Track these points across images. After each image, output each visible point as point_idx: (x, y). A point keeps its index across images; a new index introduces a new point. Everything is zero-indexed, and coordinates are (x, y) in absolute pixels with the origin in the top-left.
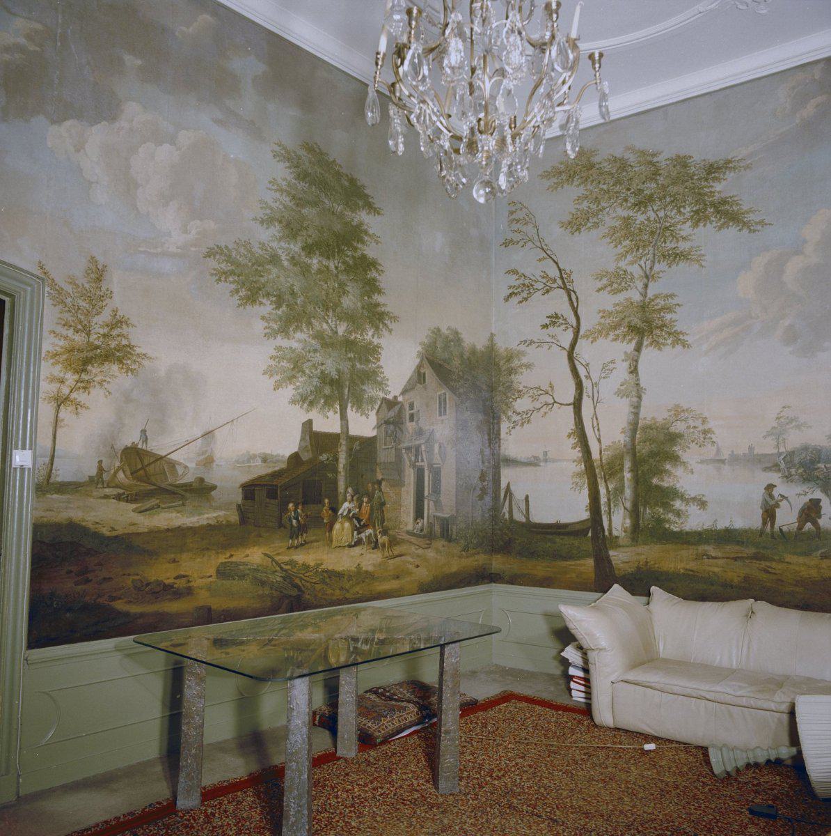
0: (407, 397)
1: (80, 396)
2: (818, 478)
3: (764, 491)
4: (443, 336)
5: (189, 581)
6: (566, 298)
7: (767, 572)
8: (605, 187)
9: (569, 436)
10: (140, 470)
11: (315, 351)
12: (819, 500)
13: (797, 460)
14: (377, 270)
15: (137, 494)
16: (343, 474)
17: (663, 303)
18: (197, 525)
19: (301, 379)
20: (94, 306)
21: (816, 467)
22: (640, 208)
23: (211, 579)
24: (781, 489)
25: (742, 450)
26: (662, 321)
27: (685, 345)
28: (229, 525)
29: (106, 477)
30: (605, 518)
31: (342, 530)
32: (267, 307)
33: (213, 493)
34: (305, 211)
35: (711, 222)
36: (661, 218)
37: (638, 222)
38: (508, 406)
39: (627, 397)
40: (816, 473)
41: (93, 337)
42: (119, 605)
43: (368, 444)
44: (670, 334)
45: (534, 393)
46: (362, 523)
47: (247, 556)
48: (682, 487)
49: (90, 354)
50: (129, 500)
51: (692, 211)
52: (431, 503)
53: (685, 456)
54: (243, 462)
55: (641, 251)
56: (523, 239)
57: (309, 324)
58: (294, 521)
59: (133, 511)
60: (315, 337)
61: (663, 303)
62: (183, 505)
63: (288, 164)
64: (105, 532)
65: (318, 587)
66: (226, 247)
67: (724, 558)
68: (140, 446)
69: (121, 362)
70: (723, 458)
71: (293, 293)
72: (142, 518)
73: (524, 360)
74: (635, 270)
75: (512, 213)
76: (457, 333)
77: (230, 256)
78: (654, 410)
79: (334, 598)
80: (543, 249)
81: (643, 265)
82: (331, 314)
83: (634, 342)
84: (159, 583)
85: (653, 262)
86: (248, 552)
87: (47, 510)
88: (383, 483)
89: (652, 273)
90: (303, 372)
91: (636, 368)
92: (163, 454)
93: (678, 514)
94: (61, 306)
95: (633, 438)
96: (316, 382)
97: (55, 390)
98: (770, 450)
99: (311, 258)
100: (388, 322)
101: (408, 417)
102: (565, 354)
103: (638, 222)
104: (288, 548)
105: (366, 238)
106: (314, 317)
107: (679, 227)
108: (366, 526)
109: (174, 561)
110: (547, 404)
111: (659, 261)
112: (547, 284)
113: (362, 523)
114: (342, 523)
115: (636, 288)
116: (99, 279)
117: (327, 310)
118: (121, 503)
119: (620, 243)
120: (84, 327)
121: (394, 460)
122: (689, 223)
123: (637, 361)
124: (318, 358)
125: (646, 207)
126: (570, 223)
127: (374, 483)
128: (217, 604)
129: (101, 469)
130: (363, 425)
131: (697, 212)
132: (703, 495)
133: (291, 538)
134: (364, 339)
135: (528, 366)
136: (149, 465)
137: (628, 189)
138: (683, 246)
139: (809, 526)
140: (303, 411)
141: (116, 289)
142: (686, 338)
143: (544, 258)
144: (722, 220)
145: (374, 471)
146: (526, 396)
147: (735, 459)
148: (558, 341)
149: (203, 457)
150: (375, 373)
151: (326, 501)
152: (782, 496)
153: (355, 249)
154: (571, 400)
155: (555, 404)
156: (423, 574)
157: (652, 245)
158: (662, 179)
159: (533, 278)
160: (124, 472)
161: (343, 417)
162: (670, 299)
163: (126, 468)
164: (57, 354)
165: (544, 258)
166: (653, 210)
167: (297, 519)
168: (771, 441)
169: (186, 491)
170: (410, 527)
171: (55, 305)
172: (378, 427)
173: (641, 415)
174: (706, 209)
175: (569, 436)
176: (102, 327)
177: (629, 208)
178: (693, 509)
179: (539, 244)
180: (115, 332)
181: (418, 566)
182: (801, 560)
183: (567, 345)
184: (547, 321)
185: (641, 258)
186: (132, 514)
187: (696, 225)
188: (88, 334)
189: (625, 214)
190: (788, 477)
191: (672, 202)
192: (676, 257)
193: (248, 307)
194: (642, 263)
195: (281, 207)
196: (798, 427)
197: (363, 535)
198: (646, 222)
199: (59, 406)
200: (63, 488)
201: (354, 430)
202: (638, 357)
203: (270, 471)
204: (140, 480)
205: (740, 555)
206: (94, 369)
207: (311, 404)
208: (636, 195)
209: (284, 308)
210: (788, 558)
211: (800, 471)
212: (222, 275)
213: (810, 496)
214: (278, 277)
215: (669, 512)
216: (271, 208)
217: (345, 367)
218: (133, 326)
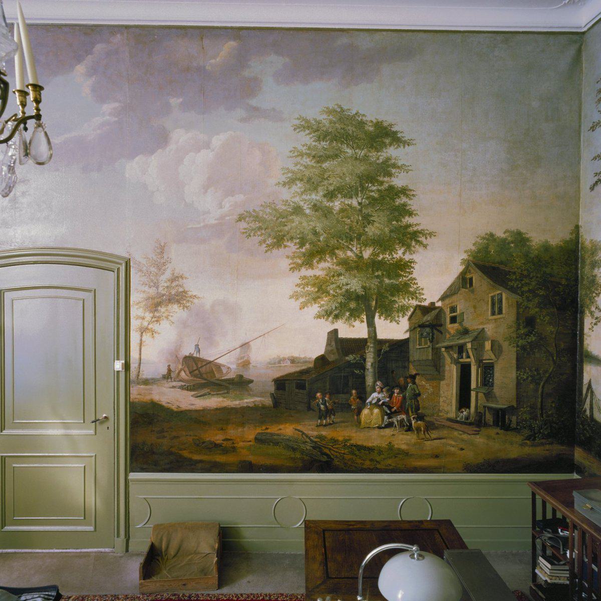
0: (447, 301)
1: (155, 326)
5: (233, 443)
10: (195, 370)
15: (194, 386)
16: (371, 370)
18: (239, 407)
19: (326, 299)
23: (250, 443)
28: (264, 407)
29: (173, 375)
32: (292, 247)
33: (250, 385)
34: (326, 165)
41: (161, 289)
42: (185, 454)
43: (399, 347)
47: (280, 429)
49: (159, 300)
50: (188, 389)
52: (480, 395)
57: (333, 254)
58: (322, 406)
59: (192, 396)
60: (338, 264)
62: (227, 393)
63: (307, 132)
64: (174, 408)
65: (347, 457)
66: (254, 211)
71: (315, 233)
72: (198, 400)
77: (257, 217)
79: (364, 467)
82: (355, 243)
84: (211, 443)
86: (281, 427)
88: (418, 377)
92: (211, 359)
97: (139, 324)
99: (332, 202)
105: (393, 171)
106: (338, 249)
114: (371, 410)
116: (162, 253)
118: (184, 391)
121: (430, 358)
124: (343, 280)
129: (169, 371)
130: (394, 329)
133: (320, 418)
136: (202, 367)
149: (242, 360)
156: (469, 455)
160: (184, 371)
161: (371, 324)
163: (186, 369)
164: (140, 302)
167: (325, 404)
169: (229, 384)
170: (452, 415)
172: (411, 330)
176: (166, 282)
180: (174, 284)
181: (462, 449)
188: (157, 288)
193: (275, 251)
195: (301, 168)
197: (394, 420)
199: (142, 333)
200: (146, 382)
201: (381, 335)
204: (195, 376)
206: (162, 309)
207: (337, 317)
209: (307, 246)
217: (373, 284)
218: (186, 278)
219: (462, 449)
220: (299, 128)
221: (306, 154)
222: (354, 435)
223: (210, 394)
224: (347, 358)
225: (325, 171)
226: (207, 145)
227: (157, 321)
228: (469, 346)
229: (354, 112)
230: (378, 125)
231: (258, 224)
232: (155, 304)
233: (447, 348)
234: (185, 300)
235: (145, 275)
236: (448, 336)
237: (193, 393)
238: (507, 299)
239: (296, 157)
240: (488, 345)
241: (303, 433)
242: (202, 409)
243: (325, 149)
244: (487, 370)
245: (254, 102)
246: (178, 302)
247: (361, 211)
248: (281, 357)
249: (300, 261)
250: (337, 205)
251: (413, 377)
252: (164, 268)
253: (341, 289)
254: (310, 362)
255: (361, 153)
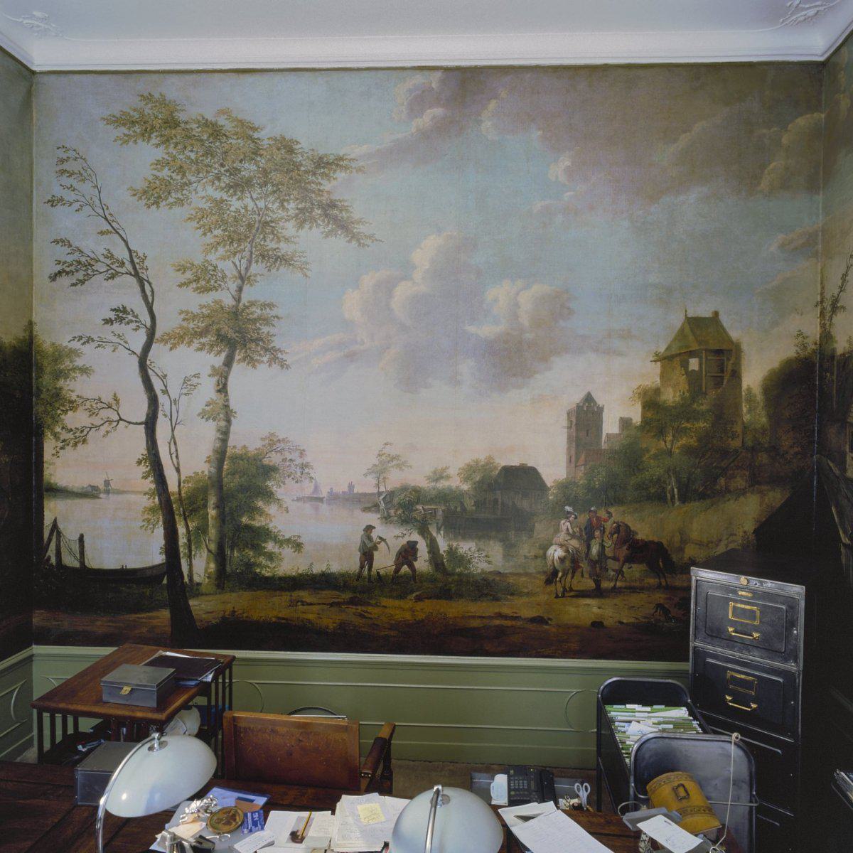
2: (416, 520)
3: (363, 532)
6: (137, 289)
7: (361, 615)
8: (193, 156)
9: (139, 463)
12: (416, 543)
13: (396, 500)
17: (259, 311)
21: (414, 508)
22: (235, 191)
24: (380, 530)
25: (342, 488)
26: (258, 333)
27: (283, 365)
30: (184, 562)
35: (318, 226)
36: (261, 209)
37: (233, 209)
38: (56, 420)
39: (214, 419)
40: (415, 515)
44: (267, 350)
45: (91, 406)
48: (276, 527)
51: (297, 209)
53: (279, 492)
55: (235, 245)
56: (78, 201)
61: (259, 311)
67: (319, 604)
70: (321, 496)
73: (79, 362)
74: (227, 267)
75: (62, 161)
78: (246, 437)
80: (106, 219)
81: (238, 263)
83: (224, 355)
85: (250, 262)
89: (248, 274)
91: (225, 386)
93: (271, 557)
95: (220, 468)
98: (371, 489)
102: (134, 363)
103: (233, 209)
107: (281, 224)
110: (110, 421)
111: (257, 262)
112: (114, 267)
115: (228, 289)
119: (210, 230)
122: (293, 222)
123: (226, 378)
125: (242, 192)
126: (145, 192)
131: (302, 210)
132: (299, 537)
135: (85, 371)
137: (222, 165)
138: (285, 248)
139: (405, 569)
142: (284, 357)
143: (107, 232)
144: (330, 226)
146: (81, 408)
147: (334, 498)
148: (126, 342)
152: (381, 538)
154: (143, 419)
155: (121, 422)
157: (248, 240)
158: (263, 161)
159: (92, 256)
162: (268, 309)
165: (107, 232)
166: (251, 197)
168: (371, 480)
173: (231, 443)
174: (312, 209)
175: (139, 463)
177: (222, 189)
178: (287, 552)
179: (101, 212)
182: (397, 603)
183: (139, 350)
184: (112, 315)
185: (235, 254)
187: (301, 225)
189: (218, 195)
190: (386, 519)
191: (275, 192)
192: (276, 260)
194: (236, 260)
196: (399, 466)
198: (242, 211)
202: (228, 373)
205: (336, 600)
208: (231, 174)
210: (384, 601)
211: (399, 512)
213: (407, 539)
215: (260, 555)
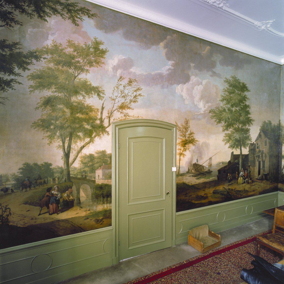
0: (257, 142)
1: (184, 153)
4: (266, 123)
5: (207, 195)
11: (234, 133)
14: (249, 108)
15: (196, 175)
16: (241, 165)
18: (209, 181)
19: (231, 141)
20: (186, 130)
23: (212, 194)
28: (215, 181)
29: (190, 171)
31: (240, 180)
32: (223, 123)
33: (212, 173)
34: (231, 95)
41: (186, 138)
42: (193, 201)
43: (247, 156)
46: (245, 177)
47: (219, 188)
49: (186, 142)
50: (195, 176)
52: (262, 170)
54: (218, 164)
57: (233, 126)
58: (229, 178)
60: (234, 129)
62: (206, 176)
63: (227, 83)
64: (190, 184)
65: (235, 195)
66: (214, 109)
68: (196, 163)
69: (192, 143)
71: (229, 119)
76: (270, 121)
77: (214, 112)
79: (239, 197)
82: (238, 122)
84: (201, 196)
86: (220, 187)
87: (179, 180)
88: (250, 166)
90: (231, 139)
92: (201, 164)
94: (180, 132)
96: (234, 141)
99: (233, 108)
100: (252, 122)
101: (257, 147)
104: (228, 185)
105: (246, 99)
106: (234, 124)
108: (246, 178)
109: (204, 190)
113: (245, 177)
114: (240, 178)
116: (187, 123)
117: (237, 121)
120: (185, 136)
121: (253, 160)
124: (235, 135)
127: (248, 166)
128: (212, 200)
129: (189, 170)
130: (246, 151)
133: (229, 183)
134: (246, 128)
136: (198, 167)
140: (231, 150)
141: (190, 125)
145: (248, 163)
149: (210, 164)
150: (248, 137)
151: (237, 172)
153: (244, 103)
156: (260, 190)
161: (241, 150)
163: (194, 169)
164: (180, 143)
167: (230, 177)
169: (206, 173)
170: (257, 177)
171: (179, 131)
172: (249, 151)
176: (188, 135)
181: (259, 188)
186: (195, 180)
188: (185, 137)
193: (219, 124)
195: (226, 96)
197: (245, 181)
199: (180, 155)
200: (182, 175)
201: (244, 153)
203: (224, 166)
206: (187, 146)
207: (233, 147)
209: (227, 123)
212: (212, 117)
214: (225, 115)
216: (223, 97)
217: (241, 136)
219: (259, 188)
220: (225, 81)
221: (227, 91)
222: (237, 187)
223: (201, 177)
224: (235, 161)
225: (231, 97)
226: (201, 83)
227: (185, 150)
228: (260, 155)
229: (238, 78)
230: (243, 84)
231: (215, 114)
232: (185, 143)
233: (256, 156)
234: (194, 142)
235: (182, 132)
236: (257, 152)
237: (196, 178)
238: (268, 141)
239: (224, 91)
240: (264, 155)
241: (225, 188)
242: (198, 183)
243: (231, 90)
244: (264, 162)
245: (214, 70)
246: (192, 143)
247: (239, 112)
248: (220, 162)
249: (225, 128)
250: (234, 109)
251: (249, 166)
252: (188, 129)
253: (234, 138)
254: (227, 163)
255: (239, 92)
